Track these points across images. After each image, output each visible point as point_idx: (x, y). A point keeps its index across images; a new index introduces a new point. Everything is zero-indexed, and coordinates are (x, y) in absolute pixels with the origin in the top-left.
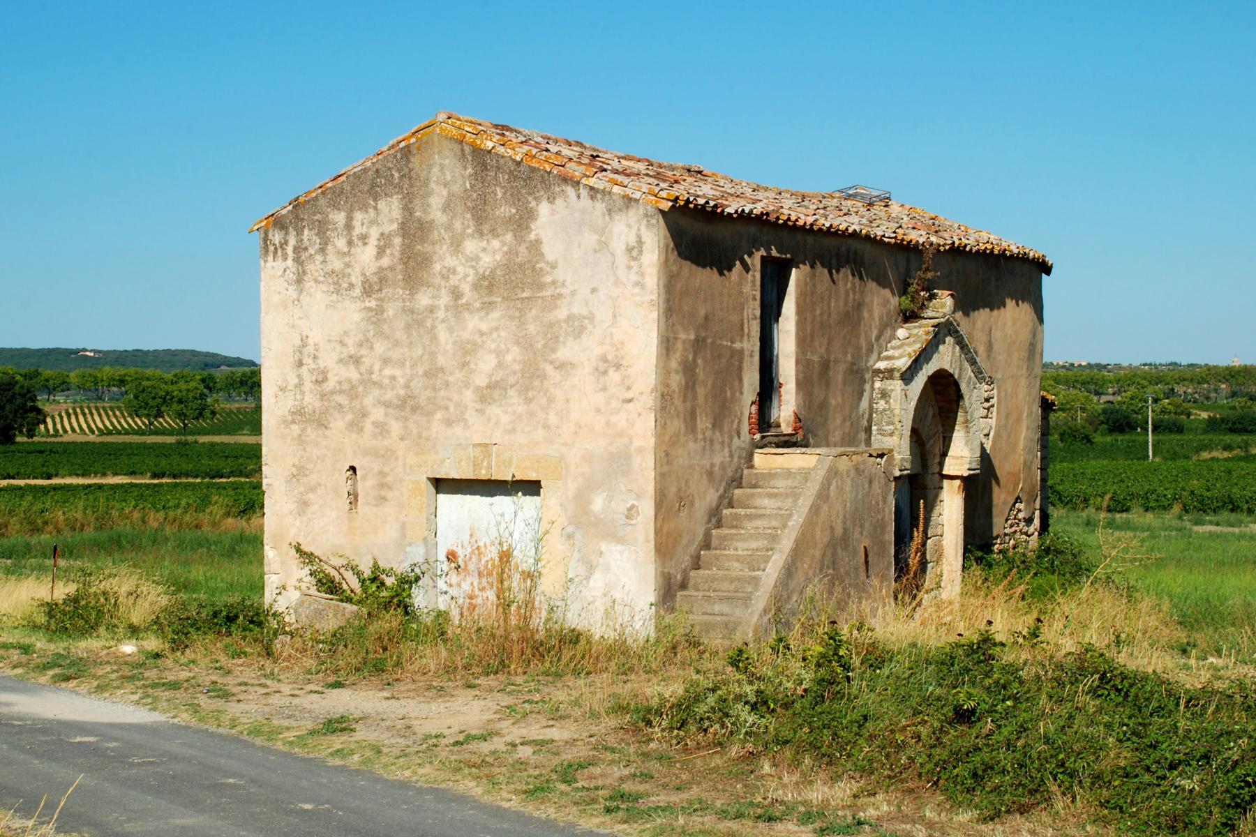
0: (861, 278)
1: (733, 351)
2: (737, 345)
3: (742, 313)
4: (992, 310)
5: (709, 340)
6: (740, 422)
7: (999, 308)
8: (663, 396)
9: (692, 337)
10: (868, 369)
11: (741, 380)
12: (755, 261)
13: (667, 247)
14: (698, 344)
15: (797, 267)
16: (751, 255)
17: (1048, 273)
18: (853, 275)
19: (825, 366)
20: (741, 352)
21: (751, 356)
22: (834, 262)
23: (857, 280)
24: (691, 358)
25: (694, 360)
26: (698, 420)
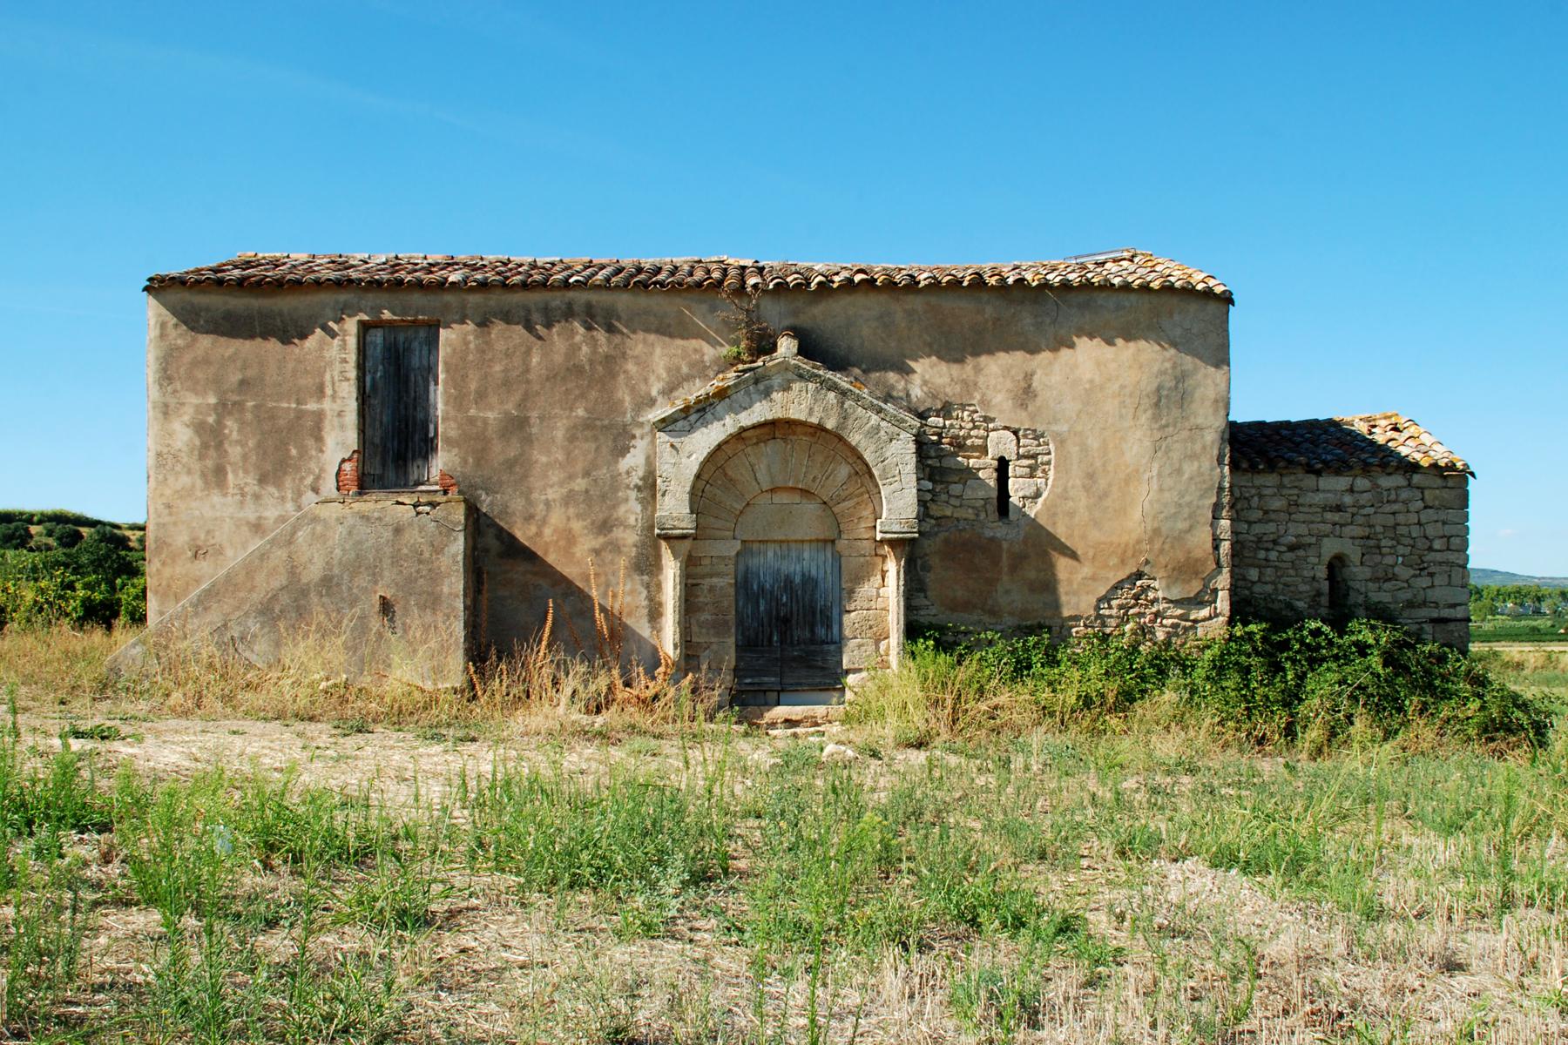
0: (611, 329)
1: (300, 415)
2: (311, 406)
3: (322, 375)
4: (1033, 350)
5: (250, 404)
6: (318, 478)
7: (1055, 349)
8: (159, 455)
9: (212, 400)
10: (641, 425)
11: (319, 439)
12: (351, 325)
13: (163, 326)
14: (223, 408)
15: (448, 326)
16: (339, 320)
17: (1231, 302)
18: (589, 328)
19: (517, 426)
20: (319, 416)
21: (340, 414)
22: (536, 317)
23: (601, 335)
24: (211, 420)
25: (219, 422)
26: (230, 476)
